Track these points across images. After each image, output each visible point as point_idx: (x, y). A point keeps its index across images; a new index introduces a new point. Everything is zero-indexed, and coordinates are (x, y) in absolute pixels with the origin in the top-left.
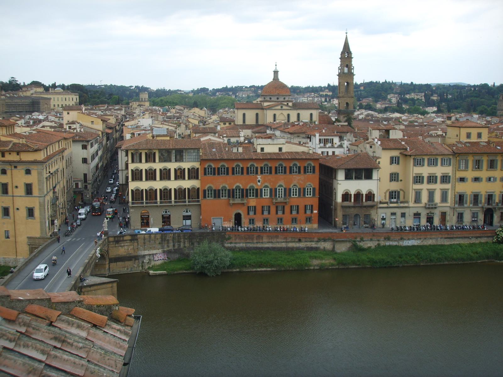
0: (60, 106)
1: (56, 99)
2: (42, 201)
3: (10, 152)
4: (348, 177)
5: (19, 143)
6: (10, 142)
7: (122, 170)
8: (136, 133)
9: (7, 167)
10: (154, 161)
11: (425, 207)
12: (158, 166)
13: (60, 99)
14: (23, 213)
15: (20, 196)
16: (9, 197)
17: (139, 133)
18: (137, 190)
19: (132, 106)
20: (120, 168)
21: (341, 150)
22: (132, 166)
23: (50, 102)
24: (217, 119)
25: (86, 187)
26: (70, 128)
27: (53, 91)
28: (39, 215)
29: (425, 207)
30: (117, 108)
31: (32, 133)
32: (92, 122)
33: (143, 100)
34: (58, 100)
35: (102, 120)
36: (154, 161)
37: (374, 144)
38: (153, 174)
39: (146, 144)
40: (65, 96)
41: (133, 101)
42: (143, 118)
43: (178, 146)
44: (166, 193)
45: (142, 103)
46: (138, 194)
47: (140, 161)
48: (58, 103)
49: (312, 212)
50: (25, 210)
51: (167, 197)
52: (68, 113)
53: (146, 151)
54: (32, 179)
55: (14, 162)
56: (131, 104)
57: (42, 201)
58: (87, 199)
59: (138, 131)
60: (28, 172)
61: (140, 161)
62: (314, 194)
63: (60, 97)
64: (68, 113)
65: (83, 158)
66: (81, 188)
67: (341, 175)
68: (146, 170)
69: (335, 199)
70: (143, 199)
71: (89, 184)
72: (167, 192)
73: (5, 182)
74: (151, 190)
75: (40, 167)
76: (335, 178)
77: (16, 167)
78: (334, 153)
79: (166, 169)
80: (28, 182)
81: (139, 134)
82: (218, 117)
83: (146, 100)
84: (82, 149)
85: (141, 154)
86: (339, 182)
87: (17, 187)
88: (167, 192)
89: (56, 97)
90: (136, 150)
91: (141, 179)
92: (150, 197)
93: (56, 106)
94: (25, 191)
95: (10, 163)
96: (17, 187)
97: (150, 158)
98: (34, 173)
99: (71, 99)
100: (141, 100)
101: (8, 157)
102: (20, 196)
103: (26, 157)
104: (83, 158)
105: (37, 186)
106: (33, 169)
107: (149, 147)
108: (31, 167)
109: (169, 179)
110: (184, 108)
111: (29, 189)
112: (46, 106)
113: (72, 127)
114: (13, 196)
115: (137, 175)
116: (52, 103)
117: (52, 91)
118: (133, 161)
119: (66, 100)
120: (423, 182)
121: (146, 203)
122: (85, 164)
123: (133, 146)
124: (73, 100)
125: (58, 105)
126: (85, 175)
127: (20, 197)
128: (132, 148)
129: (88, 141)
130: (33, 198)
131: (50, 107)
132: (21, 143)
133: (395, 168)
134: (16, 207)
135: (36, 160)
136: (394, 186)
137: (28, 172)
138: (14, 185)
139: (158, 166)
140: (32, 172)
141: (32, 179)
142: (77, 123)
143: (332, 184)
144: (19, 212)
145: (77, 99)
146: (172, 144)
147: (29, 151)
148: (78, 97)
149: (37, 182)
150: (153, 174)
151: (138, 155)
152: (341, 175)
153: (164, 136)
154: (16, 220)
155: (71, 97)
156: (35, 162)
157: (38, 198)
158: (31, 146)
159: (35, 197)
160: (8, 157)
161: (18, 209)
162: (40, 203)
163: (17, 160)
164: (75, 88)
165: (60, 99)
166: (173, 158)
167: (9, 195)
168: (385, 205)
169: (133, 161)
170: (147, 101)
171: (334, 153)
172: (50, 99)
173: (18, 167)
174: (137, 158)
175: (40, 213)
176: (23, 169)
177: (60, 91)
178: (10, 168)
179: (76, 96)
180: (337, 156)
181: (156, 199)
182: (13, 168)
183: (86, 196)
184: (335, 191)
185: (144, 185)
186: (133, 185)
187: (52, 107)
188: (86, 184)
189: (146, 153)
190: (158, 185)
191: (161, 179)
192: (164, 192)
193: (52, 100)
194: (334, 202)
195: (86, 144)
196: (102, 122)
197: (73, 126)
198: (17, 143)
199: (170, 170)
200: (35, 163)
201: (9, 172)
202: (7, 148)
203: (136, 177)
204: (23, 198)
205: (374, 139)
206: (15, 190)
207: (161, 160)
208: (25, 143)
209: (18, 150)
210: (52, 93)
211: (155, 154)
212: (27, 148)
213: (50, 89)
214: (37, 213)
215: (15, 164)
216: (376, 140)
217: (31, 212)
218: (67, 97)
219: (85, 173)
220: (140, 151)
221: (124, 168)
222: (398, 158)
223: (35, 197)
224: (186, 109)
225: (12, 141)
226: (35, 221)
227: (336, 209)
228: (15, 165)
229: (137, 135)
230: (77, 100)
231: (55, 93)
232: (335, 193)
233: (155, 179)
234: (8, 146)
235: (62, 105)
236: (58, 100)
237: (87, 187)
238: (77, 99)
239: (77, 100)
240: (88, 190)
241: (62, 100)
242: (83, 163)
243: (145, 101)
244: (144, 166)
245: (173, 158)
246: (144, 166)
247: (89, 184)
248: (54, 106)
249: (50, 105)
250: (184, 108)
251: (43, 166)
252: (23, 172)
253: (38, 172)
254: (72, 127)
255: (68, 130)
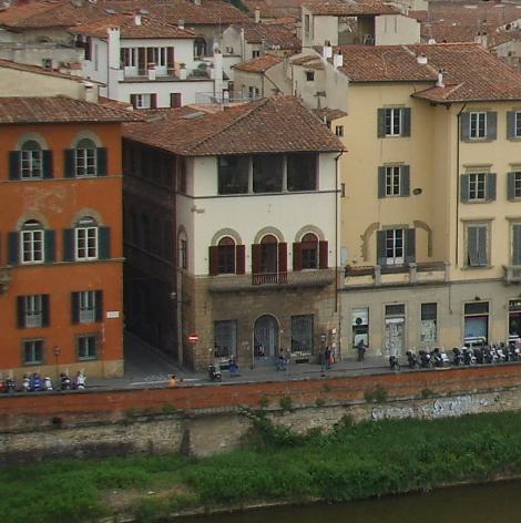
4: (230, 185)
11: (503, 282)
21: (205, 87)
29: (503, 282)
37: (320, 67)
49: (99, 317)
62: (105, 253)
67: (203, 180)
69: (185, 267)
76: (183, 190)
78: (175, 98)
86: (198, 204)
120: (492, 196)
133: (395, 150)
136: (396, 212)
143: (172, 212)
152: (203, 180)
168: (366, 280)
171: (175, 98)
180: (188, 109)
184: (182, 237)
194: (179, 276)
205: (319, 49)
216: (328, 52)
222: (407, 112)
227: (188, 303)
232: (185, 243)
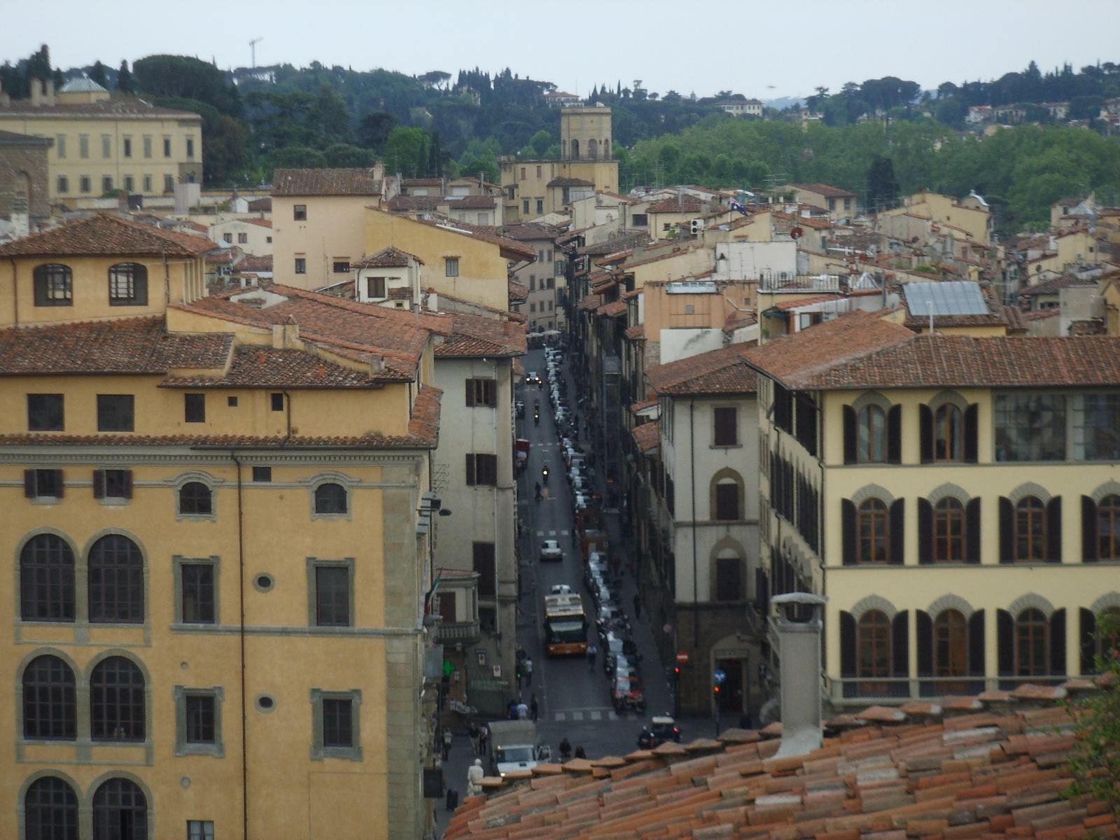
0: (97, 187)
1: (73, 146)
2: (402, 658)
3: (232, 390)
5: (269, 349)
6: (223, 339)
7: (694, 524)
8: (797, 310)
9: (219, 477)
10: (971, 456)
12: (988, 483)
13: (95, 147)
14: (296, 722)
15: (285, 632)
16: (220, 639)
17: (815, 308)
18: (874, 616)
19: (512, 188)
20: (682, 512)
22: (841, 484)
23: (44, 162)
24: (1090, 258)
25: (487, 617)
26: (376, 287)
27: (50, 100)
28: (382, 737)
30: (459, 194)
31: (259, 302)
32: (452, 261)
33: (584, 150)
34: (84, 152)
35: (505, 252)
36: (971, 456)
38: (964, 528)
39: (922, 363)
40: (127, 129)
41: (520, 160)
42: (742, 239)
43: (1102, 370)
44: (1033, 636)
45: (576, 171)
46: (874, 642)
47: (893, 456)
48: (85, 171)
50: (308, 708)
51: (1039, 659)
52: (300, 215)
53: (926, 399)
54: (358, 535)
55: (258, 445)
56: (506, 179)
57: (402, 658)
58: (490, 686)
59: (809, 302)
60: (331, 499)
61: (893, 456)
63: (95, 131)
64: (300, 215)
65: (469, 457)
66: (466, 625)
68: (923, 504)
70: (902, 668)
71: (505, 602)
72: (1039, 632)
73: (204, 554)
74: (950, 615)
75: (398, 472)
77: (262, 474)
79: (1035, 501)
80: (330, 552)
81: (816, 318)
82: (1091, 242)
83: (601, 150)
84: (469, 403)
85: (894, 417)
87: (264, 582)
88: (1039, 632)
89: (70, 131)
90: (872, 391)
91: (894, 556)
92: (943, 659)
93: (74, 189)
94: (310, 605)
95: (233, 449)
96: (264, 582)
97: (949, 439)
98: (365, 506)
99: (157, 147)
100: (568, 150)
101: (221, 420)
102: (285, 632)
103: (317, 418)
104: (469, 457)
105: (379, 575)
106: (360, 485)
107: (940, 373)
108: (348, 474)
109: (1052, 554)
110: (832, 200)
111: (331, 594)
112: (22, 183)
113: (390, 285)
114: (243, 631)
115: (872, 533)
116: (56, 166)
117: (45, 100)
118: (851, 456)
119: (128, 152)
121: (927, 690)
122: (483, 490)
123: (854, 369)
124: (167, 152)
125: (85, 184)
126: (483, 553)
127: (285, 638)
128: (847, 381)
129: (502, 361)
130: (350, 642)
131: (45, 189)
132: (278, 344)
134: (256, 690)
135: (379, 435)
137: (331, 499)
138: (252, 572)
139: (988, 483)
140: (356, 500)
141: (358, 535)
142: (412, 263)
144: (269, 719)
145: (190, 144)
146: (1069, 360)
147: (340, 388)
148: (196, 133)
149: (379, 554)
150: (964, 528)
151: (879, 421)
153: (973, 322)
154: (250, 765)
155: (157, 132)
156: (371, 447)
157: (379, 643)
158: (342, 362)
159: (365, 634)
160: (221, 420)
161: (266, 702)
162: (391, 669)
163: (272, 435)
164: (169, 82)
165: (95, 147)
166: (1076, 437)
167: (220, 627)
169: (851, 456)
170: (606, 159)
172: (43, 144)
173: (275, 475)
174: (871, 431)
175: (390, 725)
176: (302, 484)
177: (93, 98)
178: (231, 476)
179: (185, 131)
181: (978, 665)
182: (248, 475)
183: (487, 669)
185: (912, 588)
186: (847, 589)
187: (53, 193)
188: (488, 604)
189: (925, 412)
190: (989, 588)
191: (1008, 555)
192: (1024, 631)
193: (52, 153)
195: (491, 374)
196: (504, 262)
197: (398, 279)
198: (257, 349)
199: (1056, 503)
200: (377, 448)
201: (223, 501)
202: (220, 373)
203: (866, 543)
204: (301, 643)
206: (255, 597)
207: (1006, 453)
208: (299, 345)
209: (275, 380)
210: (45, 108)
211: (972, 414)
212: (323, 372)
213: (36, 86)
214: (371, 725)
215: (257, 459)
217: (336, 721)
218: (136, 131)
219: (481, 538)
220: (894, 400)
221: (704, 514)
223: (365, 634)
224: (840, 205)
225: (233, 335)
226: (357, 767)
228: (262, 463)
229: (807, 321)
230: (190, 152)
231: (60, 107)
233: (972, 556)
234: (222, 363)
235: (107, 181)
236: (84, 152)
237: (493, 622)
238: (190, 144)
239: (190, 152)
240: (499, 637)
241: (107, 154)
242: (470, 482)
243: (593, 158)
244: (911, 483)
245: (1076, 437)
246: (911, 483)
247: (505, 602)
248: (63, 184)
249: (44, 178)
250: (832, 200)
251: (417, 470)
252: (306, 499)
253: (384, 498)
254: (390, 285)
255: (364, 297)
